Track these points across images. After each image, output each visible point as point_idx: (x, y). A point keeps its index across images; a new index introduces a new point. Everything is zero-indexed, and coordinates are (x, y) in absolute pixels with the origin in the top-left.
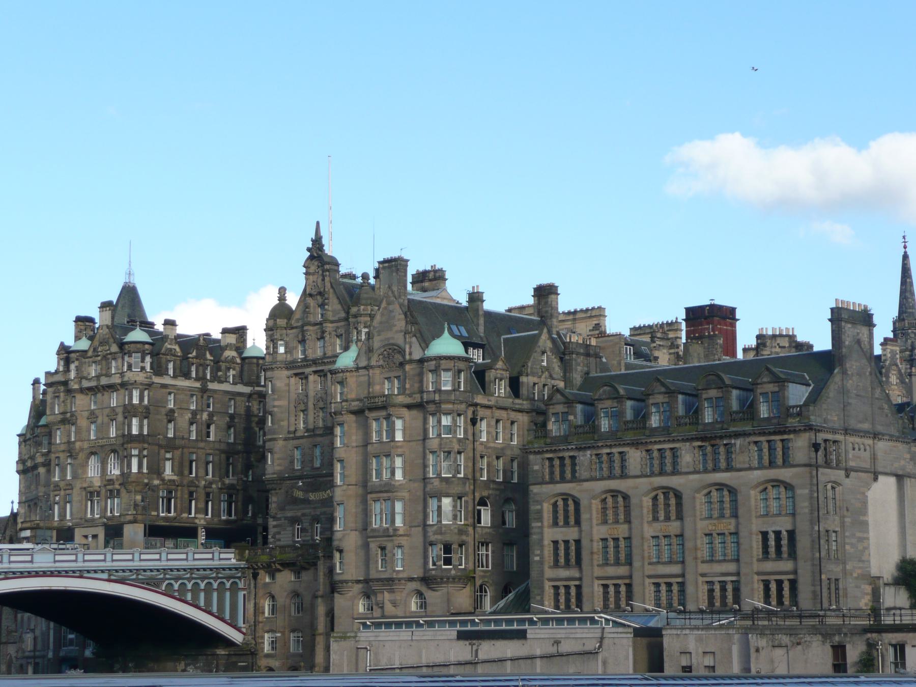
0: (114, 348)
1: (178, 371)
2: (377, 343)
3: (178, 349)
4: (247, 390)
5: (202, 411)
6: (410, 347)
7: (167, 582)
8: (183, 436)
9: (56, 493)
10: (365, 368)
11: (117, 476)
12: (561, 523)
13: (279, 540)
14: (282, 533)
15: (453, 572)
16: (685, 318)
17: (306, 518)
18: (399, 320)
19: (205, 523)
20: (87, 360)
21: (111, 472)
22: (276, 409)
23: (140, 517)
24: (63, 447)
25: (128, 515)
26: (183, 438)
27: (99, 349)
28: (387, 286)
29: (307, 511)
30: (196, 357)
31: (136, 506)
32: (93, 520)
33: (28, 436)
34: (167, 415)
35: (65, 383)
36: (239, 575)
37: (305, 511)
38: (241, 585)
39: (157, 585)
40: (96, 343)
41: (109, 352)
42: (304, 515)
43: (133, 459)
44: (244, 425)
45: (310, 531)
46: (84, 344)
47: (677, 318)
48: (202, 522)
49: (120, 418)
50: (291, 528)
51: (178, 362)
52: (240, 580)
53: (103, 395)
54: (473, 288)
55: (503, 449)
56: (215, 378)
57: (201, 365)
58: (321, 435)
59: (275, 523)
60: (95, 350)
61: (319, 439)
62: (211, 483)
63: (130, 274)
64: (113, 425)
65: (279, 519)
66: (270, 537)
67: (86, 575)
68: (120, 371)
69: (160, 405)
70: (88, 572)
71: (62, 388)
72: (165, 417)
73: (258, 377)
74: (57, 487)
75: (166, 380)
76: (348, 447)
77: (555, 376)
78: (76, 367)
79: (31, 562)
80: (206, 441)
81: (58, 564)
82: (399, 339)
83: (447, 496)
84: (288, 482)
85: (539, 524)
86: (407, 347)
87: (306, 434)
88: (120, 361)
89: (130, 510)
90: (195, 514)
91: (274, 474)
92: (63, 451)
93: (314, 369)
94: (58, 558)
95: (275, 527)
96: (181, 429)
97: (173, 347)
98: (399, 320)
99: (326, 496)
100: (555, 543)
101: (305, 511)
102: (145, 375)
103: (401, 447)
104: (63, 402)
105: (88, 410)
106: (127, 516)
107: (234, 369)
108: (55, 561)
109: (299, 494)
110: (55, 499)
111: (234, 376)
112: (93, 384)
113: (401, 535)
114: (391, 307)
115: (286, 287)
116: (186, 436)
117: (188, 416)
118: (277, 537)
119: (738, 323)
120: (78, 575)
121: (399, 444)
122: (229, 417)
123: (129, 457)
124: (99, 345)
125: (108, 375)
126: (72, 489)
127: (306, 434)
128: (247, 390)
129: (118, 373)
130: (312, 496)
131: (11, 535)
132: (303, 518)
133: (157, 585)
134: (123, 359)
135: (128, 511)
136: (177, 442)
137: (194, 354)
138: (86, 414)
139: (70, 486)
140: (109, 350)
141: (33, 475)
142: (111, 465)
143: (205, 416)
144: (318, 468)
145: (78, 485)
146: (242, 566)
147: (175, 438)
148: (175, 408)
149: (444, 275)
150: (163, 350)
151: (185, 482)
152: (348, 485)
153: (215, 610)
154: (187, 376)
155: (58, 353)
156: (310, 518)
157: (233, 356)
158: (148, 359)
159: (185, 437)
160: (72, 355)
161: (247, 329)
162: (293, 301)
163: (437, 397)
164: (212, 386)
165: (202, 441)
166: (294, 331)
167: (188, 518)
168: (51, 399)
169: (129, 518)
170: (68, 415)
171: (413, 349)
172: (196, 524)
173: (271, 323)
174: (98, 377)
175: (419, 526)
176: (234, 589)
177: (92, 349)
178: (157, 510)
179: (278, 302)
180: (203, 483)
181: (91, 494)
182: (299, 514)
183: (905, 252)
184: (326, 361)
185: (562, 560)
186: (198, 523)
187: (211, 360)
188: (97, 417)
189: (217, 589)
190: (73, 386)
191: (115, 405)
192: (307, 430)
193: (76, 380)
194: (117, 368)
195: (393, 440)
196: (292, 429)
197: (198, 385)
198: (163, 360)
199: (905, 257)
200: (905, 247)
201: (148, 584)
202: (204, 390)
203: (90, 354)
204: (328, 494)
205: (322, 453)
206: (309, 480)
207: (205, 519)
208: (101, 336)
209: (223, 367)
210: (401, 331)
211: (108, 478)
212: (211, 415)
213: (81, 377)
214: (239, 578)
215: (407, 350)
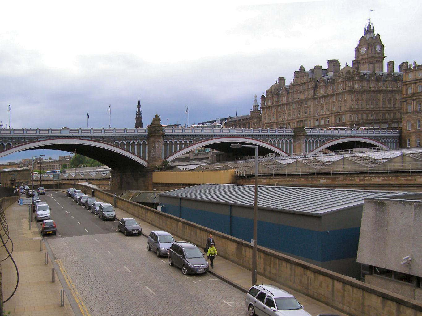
36: (291, 138)
70: (246, 136)
81: (237, 133)
94: (237, 131)
120: (242, 137)
133: (266, 141)
153: (284, 150)
176: (290, 143)
214: (292, 139)
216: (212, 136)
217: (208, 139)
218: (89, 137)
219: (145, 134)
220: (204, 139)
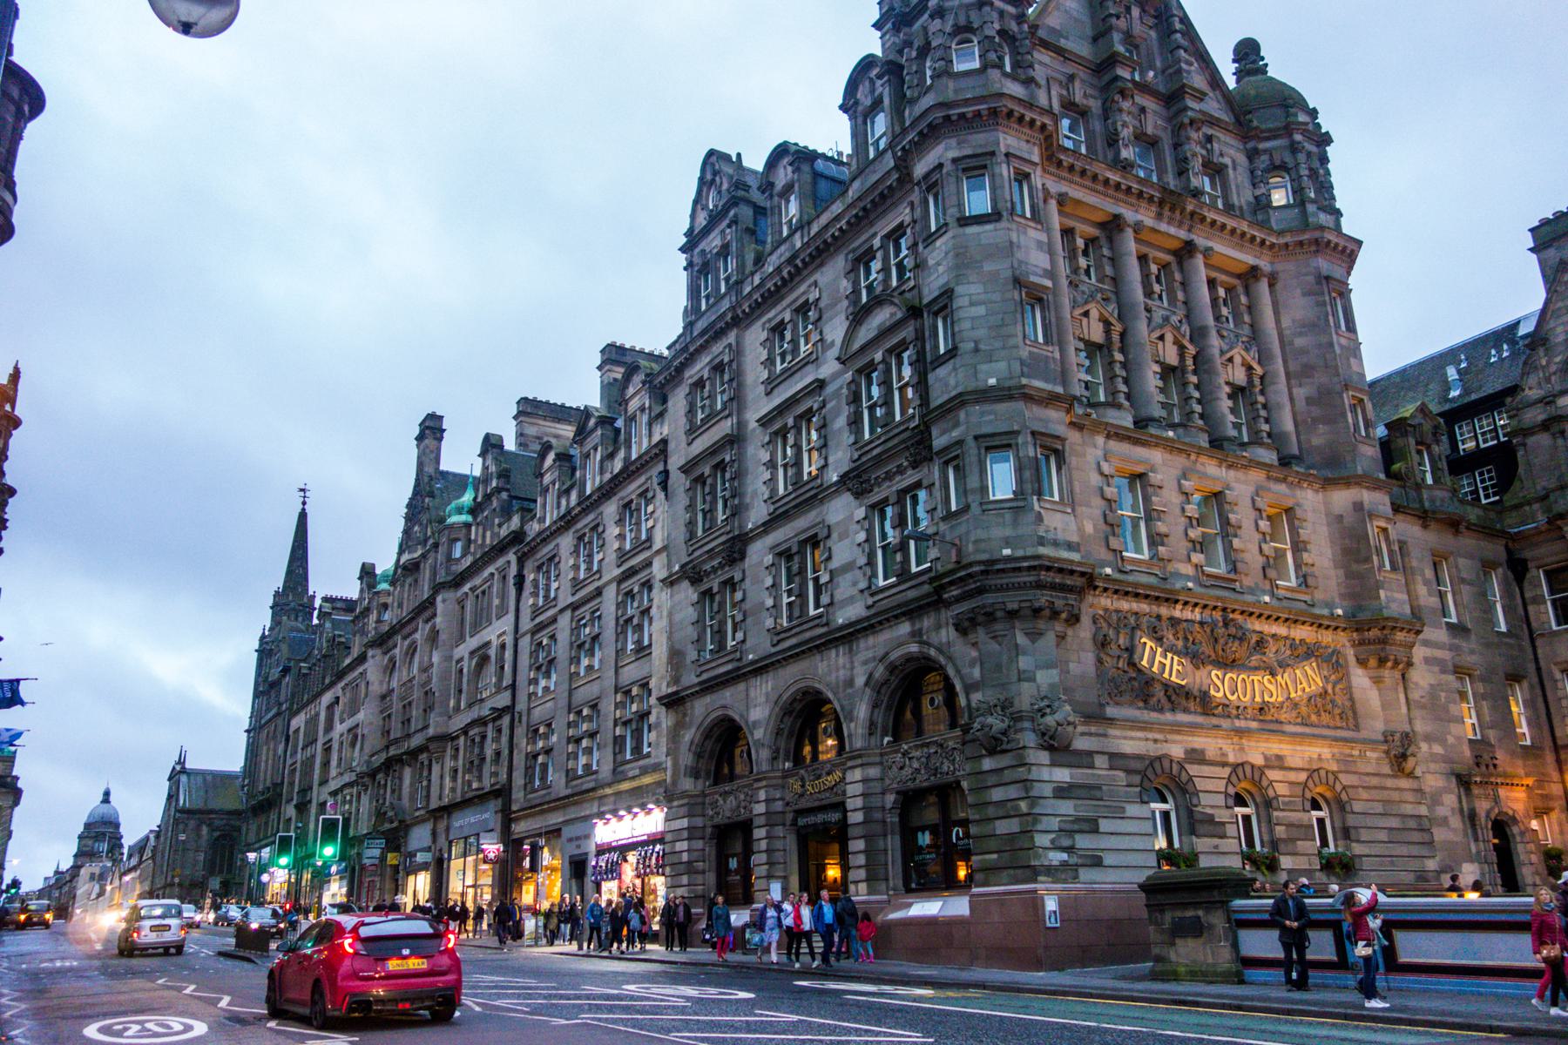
13: (1097, 862)
14: (1105, 825)
17: (1206, 770)
29: (1210, 744)
37: (1198, 742)
59: (1063, 775)
65: (1084, 759)
66: (1042, 840)
95: (1062, 792)
101: (1198, 742)
118: (1083, 842)
132: (1193, 770)
182: (1177, 751)
183: (304, 509)
199: (303, 516)
200: (304, 503)
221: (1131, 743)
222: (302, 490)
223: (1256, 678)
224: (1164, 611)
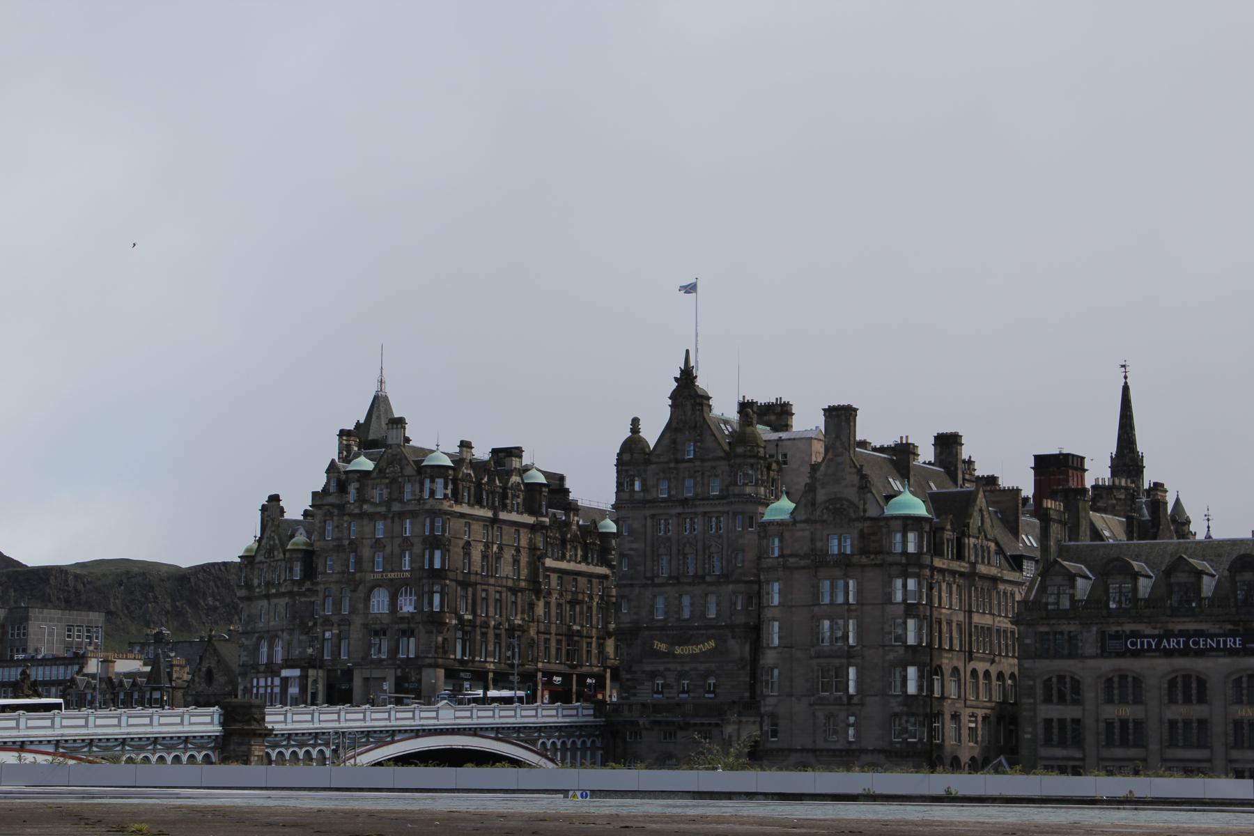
0: (409, 470)
1: (472, 498)
2: (821, 496)
3: (473, 475)
4: (530, 520)
5: (493, 543)
6: (865, 504)
7: (541, 741)
8: (477, 571)
9: (326, 628)
10: (806, 521)
11: (412, 613)
12: (1055, 698)
13: (635, 695)
14: (638, 687)
15: (919, 746)
16: (1033, 466)
18: (850, 473)
19: (494, 668)
20: (370, 481)
21: (401, 609)
22: (629, 552)
23: (440, 661)
24: (336, 577)
25: (427, 657)
26: (477, 574)
27: (387, 471)
28: (834, 436)
30: (488, 483)
31: (437, 648)
32: (381, 661)
33: (259, 558)
34: (463, 548)
35: (341, 507)
36: (597, 733)
38: (598, 744)
39: (534, 742)
40: (383, 464)
41: (400, 474)
42: (667, 670)
43: (435, 594)
44: (527, 559)
45: (676, 687)
46: (364, 464)
47: (970, 457)
48: (492, 667)
49: (417, 549)
50: (651, 683)
51: (473, 489)
52: (598, 739)
53: (393, 522)
54: (901, 438)
55: (951, 614)
56: (504, 507)
57: (492, 492)
58: (690, 584)
59: (629, 676)
60: (380, 471)
61: (688, 588)
62: (500, 624)
63: (381, 382)
64: (405, 557)
67: (482, 733)
68: (417, 497)
69: (458, 536)
71: (336, 512)
72: (462, 550)
73: (540, 506)
74: (327, 622)
75: (465, 509)
76: (784, 606)
77: (989, 536)
78: (357, 489)
79: (437, 718)
80: (495, 577)
82: (852, 494)
83: (913, 664)
84: (647, 633)
85: (1032, 701)
86: (862, 502)
87: (671, 582)
88: (417, 486)
89: (430, 653)
90: (486, 657)
91: (630, 623)
92: (336, 582)
93: (679, 510)
95: (628, 680)
96: (475, 563)
97: (469, 472)
98: (850, 473)
99: (698, 651)
100: (1048, 722)
101: (669, 666)
102: (448, 504)
103: (856, 610)
104: (338, 527)
105: (371, 538)
106: (427, 659)
107: (518, 497)
108: (456, 718)
109: (663, 647)
110: (324, 635)
111: (518, 504)
112: (383, 509)
113: (855, 704)
114: (839, 459)
115: (639, 417)
116: (479, 571)
117: (481, 547)
119: (1086, 473)
121: (853, 607)
122: (515, 550)
123: (432, 593)
124: (387, 466)
125: (401, 500)
126: (350, 625)
127: (671, 582)
128: (530, 520)
129: (415, 500)
130: (678, 650)
131: (209, 666)
134: (422, 484)
135: (427, 653)
136: (473, 578)
137: (486, 479)
138: (368, 542)
139: (345, 622)
140: (401, 472)
141: (269, 604)
142: (401, 601)
143: (495, 548)
144: (687, 620)
145: (358, 621)
146: (602, 724)
147: (469, 573)
148: (470, 539)
149: (791, 409)
150: (460, 475)
151: (478, 622)
152: (784, 647)
154: (479, 502)
155: (328, 471)
156: (676, 673)
157: (518, 483)
158: (450, 487)
159: (478, 572)
160: (351, 475)
161: (516, 452)
162: (651, 434)
163: (904, 560)
164: (503, 516)
165: (492, 576)
166: (654, 466)
167: (480, 661)
168: (320, 522)
169: (428, 661)
170: (346, 542)
171: (867, 506)
172: (486, 668)
173: (627, 457)
174: (390, 500)
175: (876, 695)
177: (377, 471)
178: (455, 653)
179: (630, 434)
180: (493, 623)
181: (376, 631)
182: (661, 668)
183: (1126, 383)
184: (698, 503)
185: (1055, 738)
186: (489, 667)
187: (500, 487)
188: (385, 546)
189: (560, 749)
190: (353, 510)
191: (408, 534)
192: (670, 577)
193: (357, 504)
194: (413, 493)
195: (847, 602)
196: (649, 574)
197: (490, 514)
198: (460, 487)
199: (1126, 389)
200: (1126, 377)
201: (526, 742)
202: (495, 521)
203: (374, 475)
204: (701, 649)
205: (692, 605)
206: (675, 632)
207: (494, 662)
208: (390, 456)
209: (510, 495)
210: (853, 486)
211: (399, 615)
212: (501, 548)
213: (362, 499)
214: (597, 736)
215: (861, 507)
216: (393, 733)
217: (381, 743)
218: (49, 742)
219: (210, 728)
220: (372, 742)
221: (648, 668)
222: (1123, 366)
223: (690, 647)
224: (664, 632)
